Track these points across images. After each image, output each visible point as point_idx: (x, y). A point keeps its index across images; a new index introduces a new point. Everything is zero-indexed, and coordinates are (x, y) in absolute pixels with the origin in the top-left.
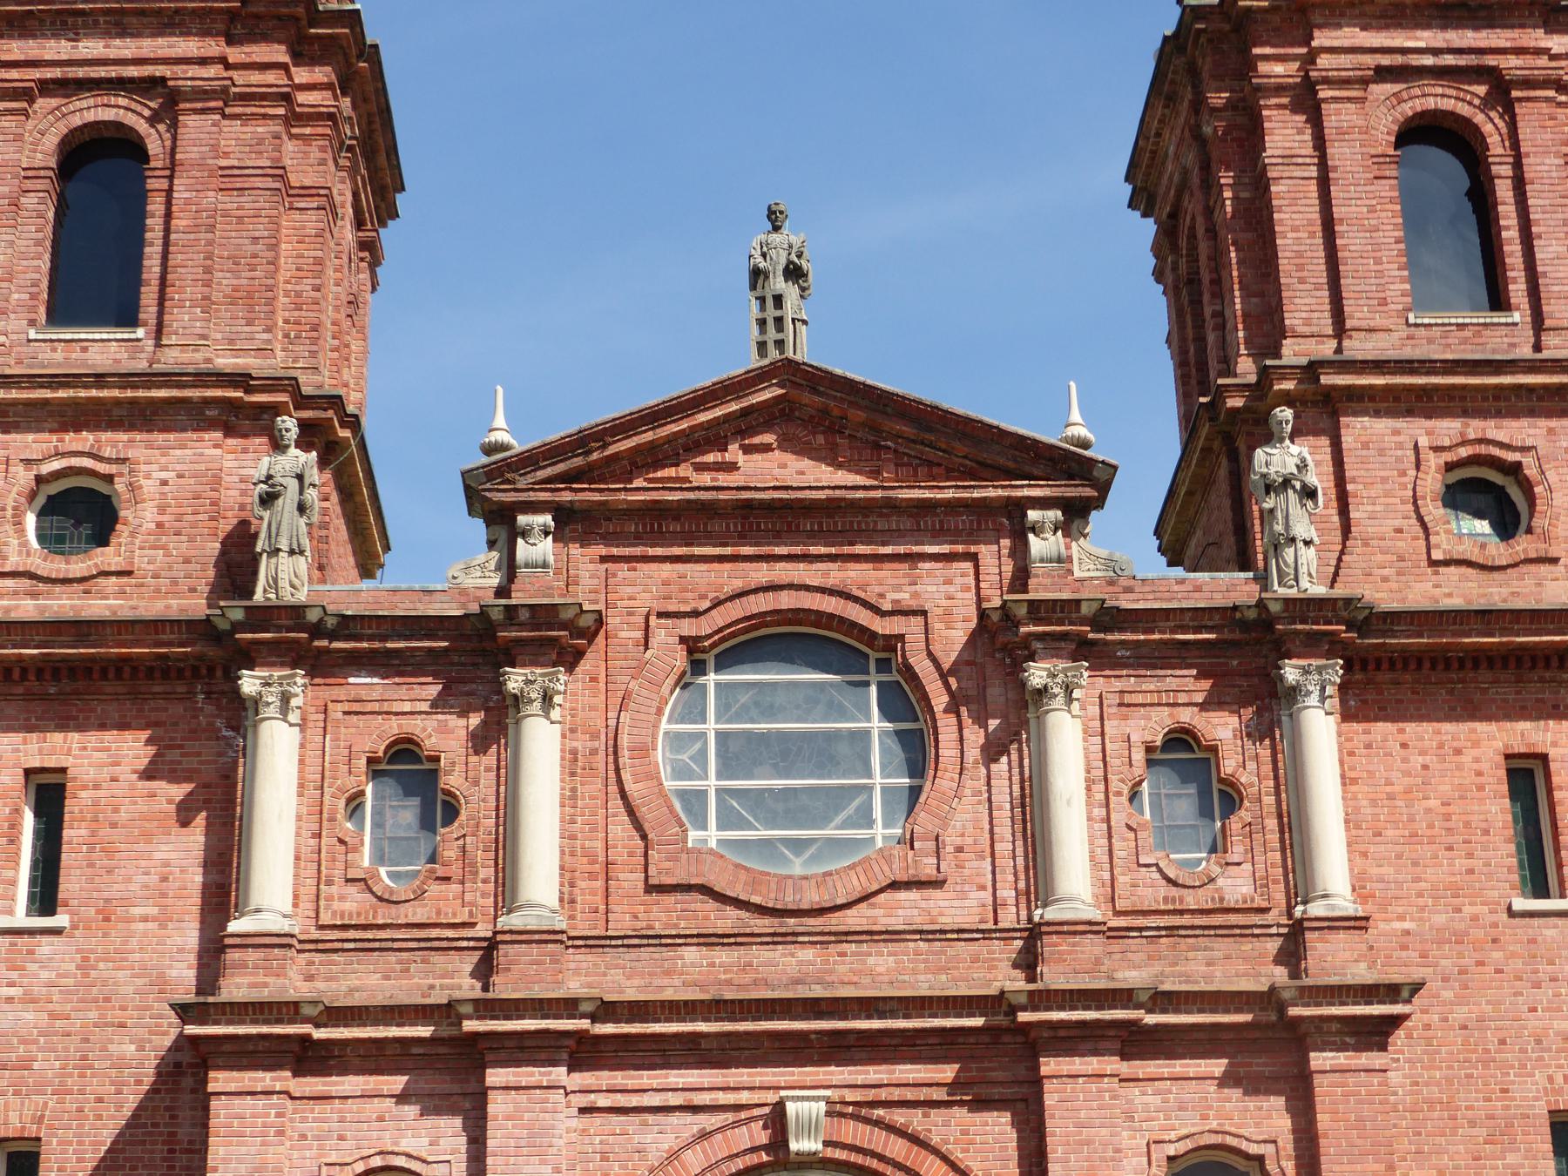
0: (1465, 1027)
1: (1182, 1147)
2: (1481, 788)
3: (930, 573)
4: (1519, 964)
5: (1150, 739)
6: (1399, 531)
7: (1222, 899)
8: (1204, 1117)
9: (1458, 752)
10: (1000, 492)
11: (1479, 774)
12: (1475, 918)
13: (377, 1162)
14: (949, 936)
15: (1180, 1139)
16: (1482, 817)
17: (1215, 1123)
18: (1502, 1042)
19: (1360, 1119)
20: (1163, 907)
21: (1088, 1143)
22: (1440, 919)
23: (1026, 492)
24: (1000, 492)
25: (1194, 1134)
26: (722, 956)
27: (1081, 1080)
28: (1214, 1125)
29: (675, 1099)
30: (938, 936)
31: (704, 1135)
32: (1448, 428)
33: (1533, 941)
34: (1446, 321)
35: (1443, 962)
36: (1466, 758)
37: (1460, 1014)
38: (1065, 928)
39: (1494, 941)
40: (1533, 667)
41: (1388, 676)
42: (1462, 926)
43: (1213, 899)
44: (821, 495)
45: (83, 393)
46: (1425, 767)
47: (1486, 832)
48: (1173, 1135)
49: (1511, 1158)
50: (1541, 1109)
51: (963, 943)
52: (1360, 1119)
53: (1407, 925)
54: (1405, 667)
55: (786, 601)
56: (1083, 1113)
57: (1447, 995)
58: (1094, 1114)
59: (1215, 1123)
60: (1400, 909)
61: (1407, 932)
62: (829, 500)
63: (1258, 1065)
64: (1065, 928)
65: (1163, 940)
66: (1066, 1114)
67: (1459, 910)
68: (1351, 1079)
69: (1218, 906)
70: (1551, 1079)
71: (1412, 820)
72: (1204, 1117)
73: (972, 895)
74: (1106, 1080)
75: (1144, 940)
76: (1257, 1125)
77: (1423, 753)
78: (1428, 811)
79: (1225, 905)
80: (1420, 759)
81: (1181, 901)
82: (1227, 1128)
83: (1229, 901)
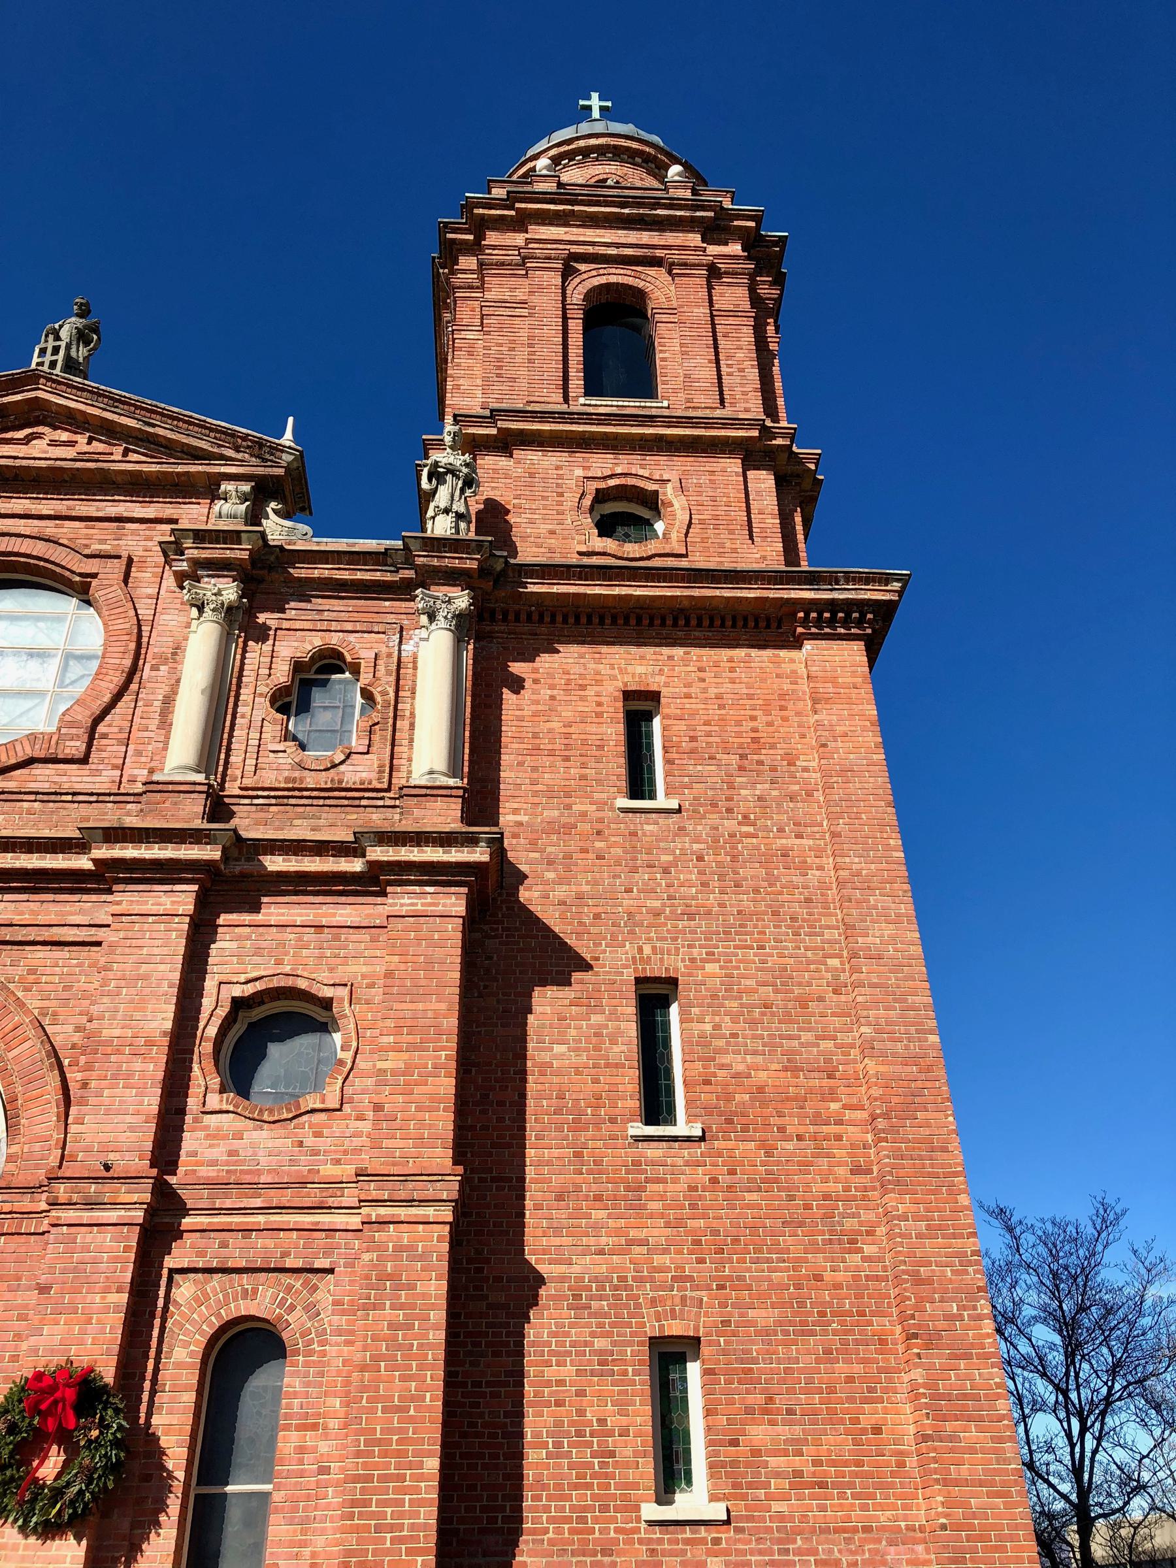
0: (564, 903)
1: (250, 989)
2: (599, 715)
3: (134, 532)
4: (619, 851)
5: (299, 655)
6: (552, 532)
7: (340, 782)
8: (279, 962)
9: (583, 687)
10: (200, 468)
11: (599, 704)
12: (584, 814)
14: (64, 798)
15: (246, 983)
16: (599, 737)
17: (289, 967)
18: (597, 916)
19: (429, 963)
20: (283, 785)
21: (145, 977)
23: (223, 469)
24: (200, 468)
25: (262, 977)
27: (151, 919)
28: (287, 969)
30: (53, 798)
32: (602, 464)
33: (634, 834)
34: (610, 403)
35: (549, 849)
36: (590, 692)
37: (560, 892)
38: (170, 787)
39: (599, 833)
40: (651, 624)
41: (527, 628)
42: (572, 820)
43: (332, 780)
44: (43, 464)
46: (553, 698)
47: (600, 747)
48: (243, 978)
49: (595, 1019)
50: (629, 975)
51: (76, 805)
52: (429, 963)
53: (518, 818)
54: (541, 620)
56: (145, 951)
57: (550, 875)
58: (156, 951)
59: (289, 967)
60: (516, 806)
61: (520, 824)
62: (49, 468)
63: (341, 915)
64: (170, 787)
65: (272, 809)
66: (127, 950)
67: (568, 807)
68: (426, 924)
69: (336, 786)
70: (640, 950)
71: (535, 736)
72: (279, 962)
73: (104, 773)
74: (177, 919)
75: (254, 808)
76: (331, 970)
77: (552, 687)
78: (550, 731)
79: (344, 785)
80: (549, 692)
81: (302, 780)
82: (299, 973)
83: (347, 782)
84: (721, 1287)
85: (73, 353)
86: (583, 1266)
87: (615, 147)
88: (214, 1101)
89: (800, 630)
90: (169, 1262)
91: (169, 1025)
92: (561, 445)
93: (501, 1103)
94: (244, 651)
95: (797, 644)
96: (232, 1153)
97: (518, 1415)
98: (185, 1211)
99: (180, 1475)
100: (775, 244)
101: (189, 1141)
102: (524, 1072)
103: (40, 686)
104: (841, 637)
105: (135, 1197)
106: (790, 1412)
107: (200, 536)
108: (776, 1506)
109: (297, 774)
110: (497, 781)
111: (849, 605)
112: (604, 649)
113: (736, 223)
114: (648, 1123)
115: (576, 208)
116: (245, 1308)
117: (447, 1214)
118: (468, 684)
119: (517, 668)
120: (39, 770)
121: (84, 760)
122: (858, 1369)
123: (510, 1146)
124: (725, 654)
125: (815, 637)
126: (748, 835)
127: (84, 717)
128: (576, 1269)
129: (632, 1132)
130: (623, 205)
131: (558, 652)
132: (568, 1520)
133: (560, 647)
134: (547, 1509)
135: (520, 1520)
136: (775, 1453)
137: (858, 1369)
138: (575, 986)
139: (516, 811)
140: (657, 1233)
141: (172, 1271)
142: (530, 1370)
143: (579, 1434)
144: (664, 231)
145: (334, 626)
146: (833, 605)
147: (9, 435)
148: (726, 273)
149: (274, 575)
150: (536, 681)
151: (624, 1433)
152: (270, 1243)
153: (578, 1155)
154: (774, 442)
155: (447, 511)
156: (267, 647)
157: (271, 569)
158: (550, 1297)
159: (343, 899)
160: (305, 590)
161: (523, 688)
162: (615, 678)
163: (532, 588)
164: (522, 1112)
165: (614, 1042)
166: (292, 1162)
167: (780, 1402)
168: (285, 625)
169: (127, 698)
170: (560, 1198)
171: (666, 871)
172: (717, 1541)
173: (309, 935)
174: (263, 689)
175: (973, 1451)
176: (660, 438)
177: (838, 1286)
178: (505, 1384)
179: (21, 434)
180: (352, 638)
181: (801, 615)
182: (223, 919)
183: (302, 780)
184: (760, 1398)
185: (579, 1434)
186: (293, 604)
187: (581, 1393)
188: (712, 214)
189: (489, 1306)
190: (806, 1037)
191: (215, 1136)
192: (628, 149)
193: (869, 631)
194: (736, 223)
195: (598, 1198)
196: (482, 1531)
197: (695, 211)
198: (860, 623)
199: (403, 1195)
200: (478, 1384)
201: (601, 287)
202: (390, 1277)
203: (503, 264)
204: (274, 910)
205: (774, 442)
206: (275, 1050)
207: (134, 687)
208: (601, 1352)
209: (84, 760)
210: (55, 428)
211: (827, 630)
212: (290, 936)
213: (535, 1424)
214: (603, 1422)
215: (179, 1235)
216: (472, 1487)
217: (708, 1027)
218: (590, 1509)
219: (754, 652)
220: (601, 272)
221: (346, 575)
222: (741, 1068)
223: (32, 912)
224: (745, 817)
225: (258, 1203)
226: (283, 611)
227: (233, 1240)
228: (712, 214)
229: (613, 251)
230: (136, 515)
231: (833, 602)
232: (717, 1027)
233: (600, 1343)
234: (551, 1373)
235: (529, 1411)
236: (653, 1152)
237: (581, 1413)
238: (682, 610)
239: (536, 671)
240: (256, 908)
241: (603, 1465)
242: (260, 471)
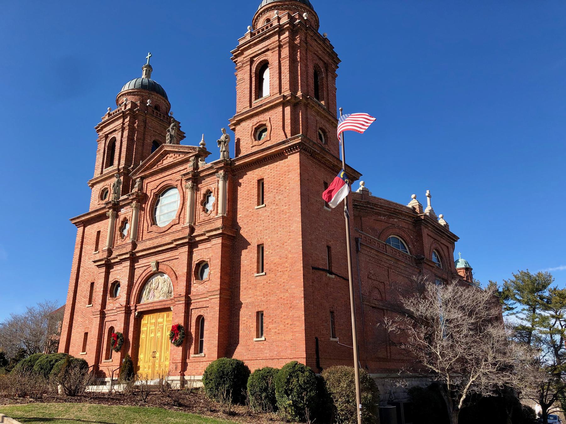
6: (247, 143)
9: (251, 182)
13: (115, 280)
22: (245, 213)
26: (151, 242)
29: (143, 265)
31: (145, 270)
33: (258, 214)
41: (241, 171)
45: (104, 177)
55: (165, 183)
76: (208, 256)
78: (245, 194)
84: (267, 302)
85: (172, 134)
86: (248, 300)
87: (266, 8)
88: (195, 282)
89: (286, 154)
90: (191, 308)
91: (186, 271)
92: (248, 119)
93: (237, 273)
94: (197, 194)
95: (286, 157)
96: (197, 290)
97: (239, 326)
98: (191, 300)
99: (194, 338)
100: (298, 24)
101: (192, 289)
102: (240, 267)
103: (175, 209)
104: (294, 153)
105: (183, 299)
106: (275, 322)
107: (184, 175)
108: (272, 337)
109: (205, 218)
110: (237, 208)
111: (293, 146)
112: (254, 171)
113: (285, 27)
114: (257, 273)
115: (251, 43)
116: (199, 314)
117: (218, 296)
118: (227, 190)
119: (240, 181)
120: (174, 227)
121: (179, 223)
122: (286, 314)
123: (238, 281)
124: (276, 164)
125: (289, 155)
126: (278, 208)
127: (178, 215)
128: (247, 301)
129: (255, 275)
130: (259, 37)
131: (247, 174)
132: (245, 341)
133: (247, 173)
134: (242, 340)
135: (239, 342)
136: (273, 329)
137: (286, 314)
138: (248, 249)
139: (240, 214)
140: (258, 293)
141: (191, 309)
142: (240, 319)
143: (247, 328)
144: (270, 38)
145: (209, 184)
146: (290, 147)
147: (164, 159)
148: (283, 45)
149: (198, 177)
150: (243, 183)
151: (252, 328)
152: (201, 303)
153: (248, 281)
154: (288, 99)
155: (222, 151)
156: (200, 192)
157: (197, 176)
158: (243, 306)
159: (208, 242)
160: (204, 178)
161: (241, 185)
162: (256, 177)
163: (237, 164)
164: (240, 275)
165: (253, 259)
166: (204, 290)
167: (274, 320)
168: (202, 186)
169: (183, 209)
170: (245, 289)
171: (263, 221)
172: (263, 343)
173: (205, 250)
174: (199, 202)
175: (298, 326)
176: (265, 109)
177: (284, 299)
178: (237, 321)
179: (165, 158)
180: (211, 186)
181: (284, 151)
182: (194, 250)
183: (205, 219)
184: (271, 320)
185: (247, 328)
186: (203, 181)
187: (247, 322)
188: (278, 29)
189: (236, 309)
190: (283, 251)
191: (195, 287)
192: (269, 7)
193: (299, 150)
194: (285, 27)
195: (250, 288)
196: (235, 344)
197: (274, 30)
198: (297, 148)
199: (213, 294)
200: (234, 322)
201: (257, 66)
202: (212, 307)
203: (240, 68)
204: (201, 246)
205: (288, 99)
206: (206, 270)
207: (184, 206)
208: (249, 315)
209: (179, 223)
210: (169, 154)
211: (291, 153)
212: (202, 251)
213: (241, 327)
214: (250, 326)
215: (191, 304)
216: (233, 337)
217: (268, 252)
218: (248, 339)
219: (281, 162)
220: (261, 57)
221: (208, 173)
222: (272, 260)
223: (172, 254)
224: (277, 204)
225: (199, 297)
226: (202, 183)
227: (198, 303)
228: (278, 29)
229: (260, 52)
230: (182, 169)
231: (289, 146)
232: (269, 252)
233: (250, 313)
234: (243, 319)
235: (240, 325)
236: (258, 278)
237: (247, 325)
238: (265, 157)
239: (243, 180)
240: (197, 247)
241: (250, 333)
242: (194, 154)
